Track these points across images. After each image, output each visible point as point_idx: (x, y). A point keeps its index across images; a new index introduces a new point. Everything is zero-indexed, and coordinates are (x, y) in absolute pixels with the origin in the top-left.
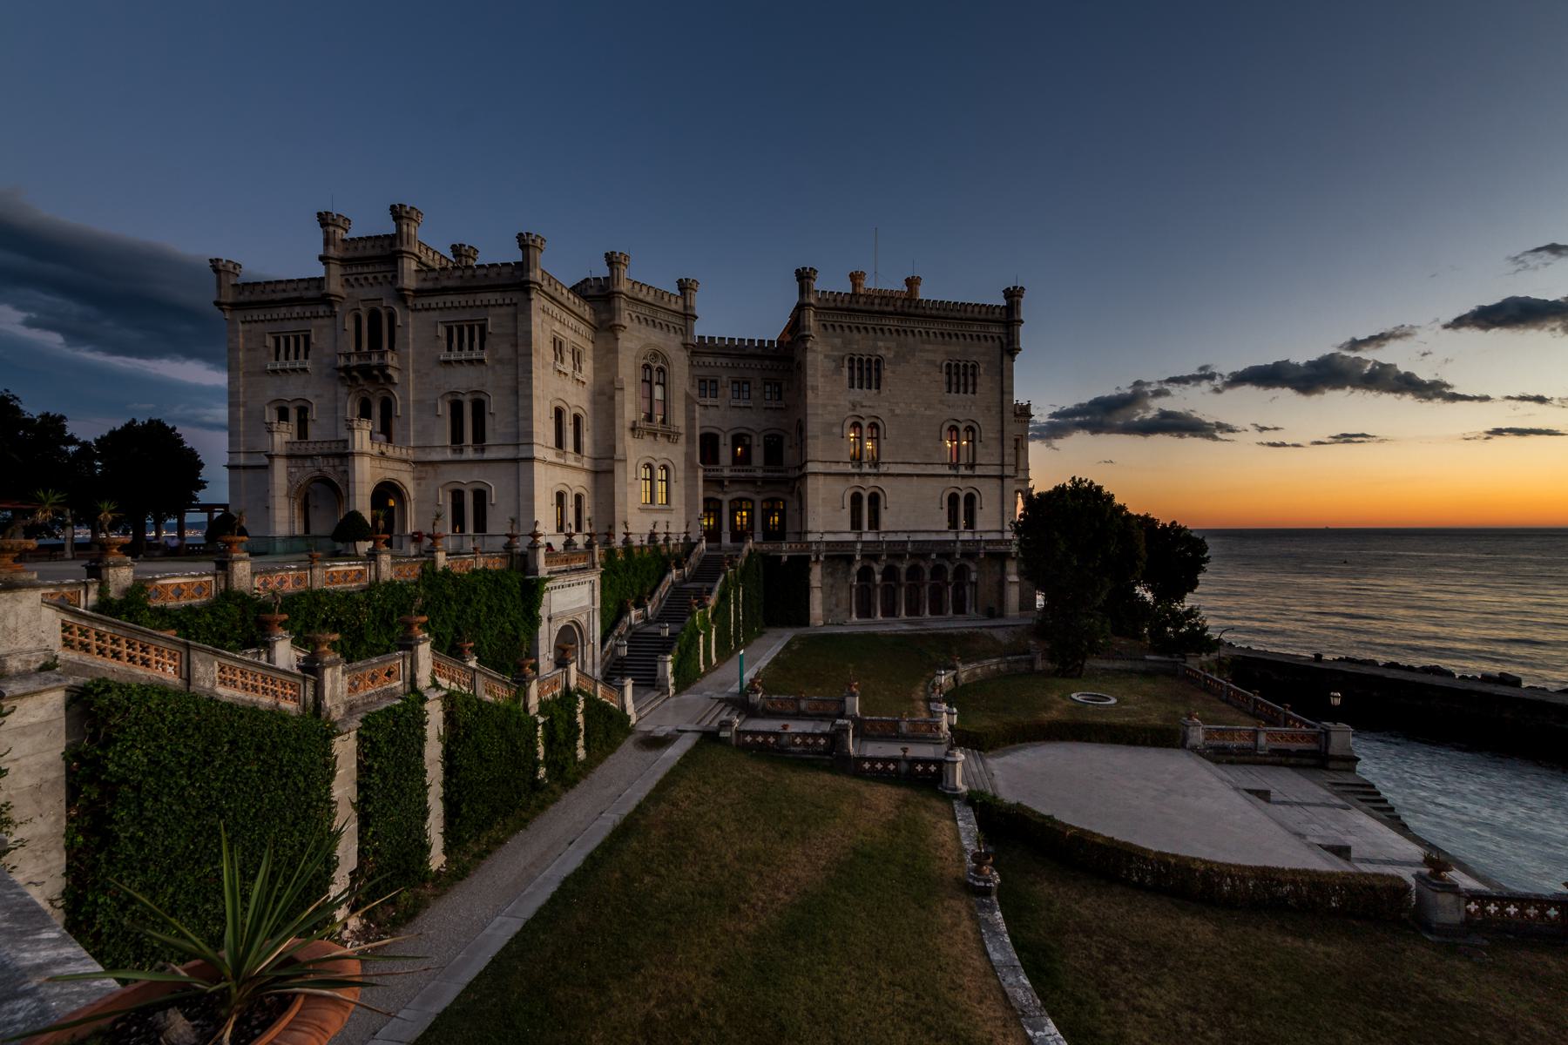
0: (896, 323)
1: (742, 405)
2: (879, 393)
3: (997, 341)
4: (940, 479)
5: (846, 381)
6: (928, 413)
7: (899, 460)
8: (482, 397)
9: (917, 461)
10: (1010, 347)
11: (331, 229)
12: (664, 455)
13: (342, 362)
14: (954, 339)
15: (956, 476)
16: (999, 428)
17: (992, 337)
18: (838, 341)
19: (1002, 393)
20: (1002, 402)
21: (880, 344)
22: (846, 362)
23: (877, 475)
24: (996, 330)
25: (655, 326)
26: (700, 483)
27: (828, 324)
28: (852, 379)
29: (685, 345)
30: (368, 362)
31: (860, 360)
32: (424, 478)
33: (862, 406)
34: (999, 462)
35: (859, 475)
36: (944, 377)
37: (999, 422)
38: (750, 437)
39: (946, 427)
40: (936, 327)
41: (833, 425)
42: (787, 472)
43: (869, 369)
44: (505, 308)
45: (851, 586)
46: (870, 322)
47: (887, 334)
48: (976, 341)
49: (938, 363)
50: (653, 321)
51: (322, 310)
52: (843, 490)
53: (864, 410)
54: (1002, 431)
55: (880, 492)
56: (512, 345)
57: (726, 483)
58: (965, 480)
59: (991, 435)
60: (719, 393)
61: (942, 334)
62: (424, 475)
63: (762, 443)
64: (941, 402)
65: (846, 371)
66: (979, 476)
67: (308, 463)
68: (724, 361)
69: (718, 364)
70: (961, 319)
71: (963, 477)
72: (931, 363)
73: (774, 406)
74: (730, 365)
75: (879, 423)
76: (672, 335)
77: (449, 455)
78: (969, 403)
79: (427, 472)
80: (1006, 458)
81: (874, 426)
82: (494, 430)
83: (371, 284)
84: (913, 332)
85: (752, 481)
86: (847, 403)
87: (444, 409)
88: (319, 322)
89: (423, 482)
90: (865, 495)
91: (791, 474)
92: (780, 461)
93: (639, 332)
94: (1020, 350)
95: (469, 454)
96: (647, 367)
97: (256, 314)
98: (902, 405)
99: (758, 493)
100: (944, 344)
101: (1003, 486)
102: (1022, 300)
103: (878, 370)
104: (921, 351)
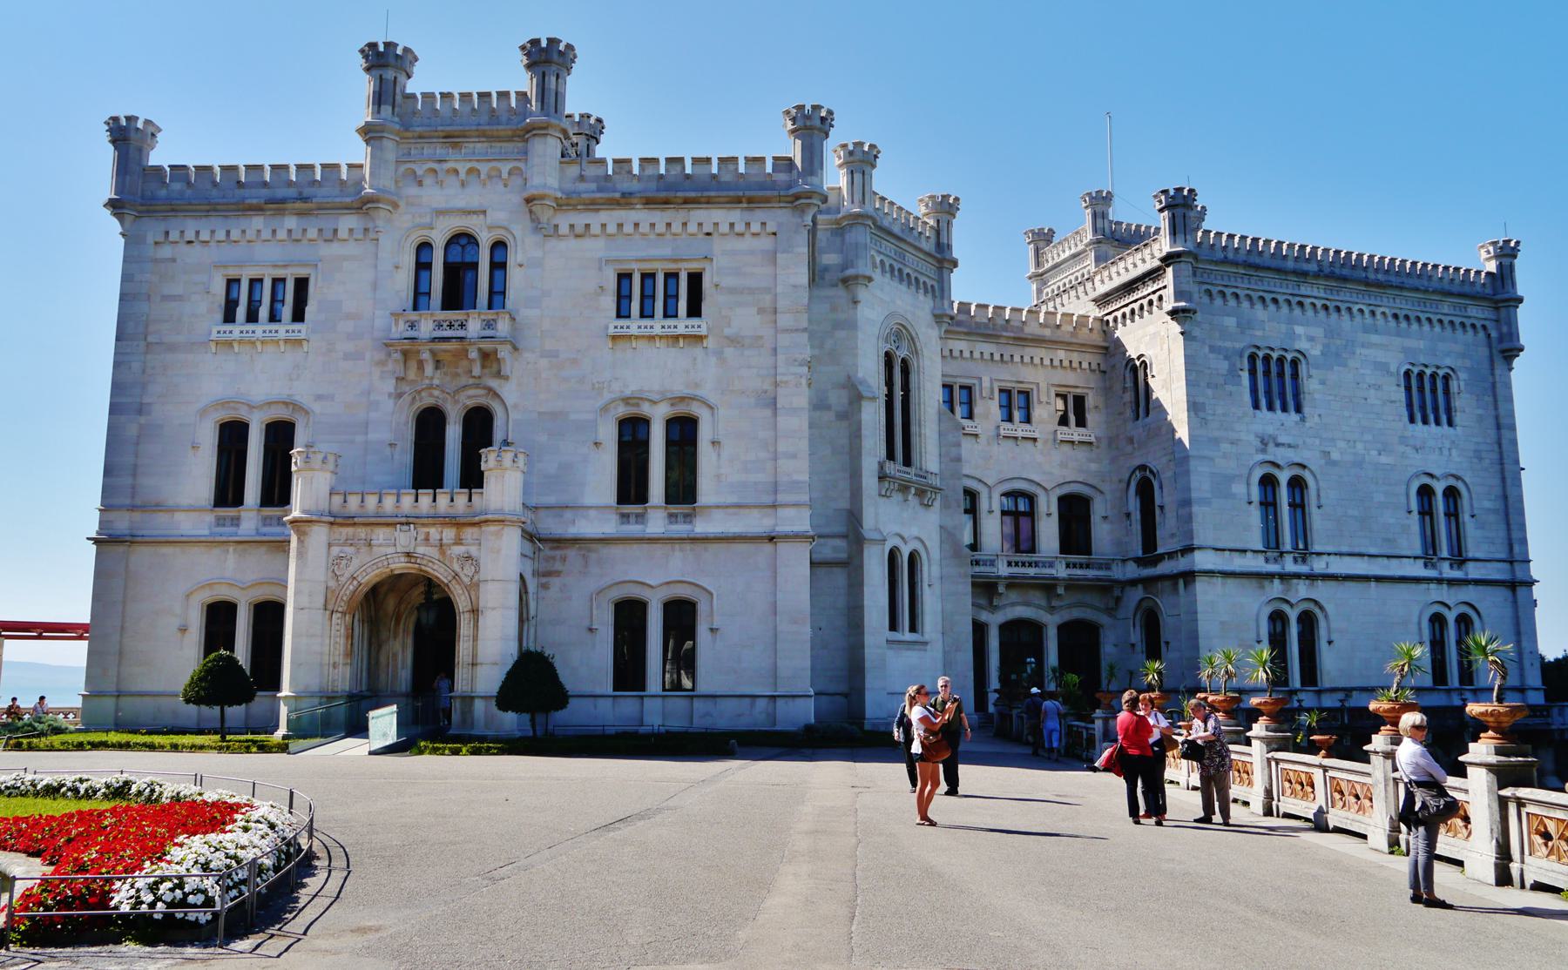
0: (1322, 294)
1: (1020, 434)
2: (1303, 419)
3: (1481, 334)
4: (1413, 586)
5: (1247, 397)
6: (1384, 459)
7: (1345, 549)
8: (696, 410)
9: (1373, 551)
10: (1505, 346)
11: (389, 74)
12: (915, 531)
13: (400, 329)
14: (1415, 326)
15: (1439, 581)
16: (1498, 491)
17: (1473, 326)
19: (1498, 427)
20: (1500, 445)
21: (1299, 330)
23: (1311, 577)
24: (1477, 312)
25: (901, 280)
26: (969, 588)
27: (1214, 290)
29: (938, 318)
30: (461, 333)
31: (1267, 358)
32: (557, 573)
33: (1278, 445)
34: (1503, 556)
35: (1284, 577)
36: (1401, 395)
37: (1497, 481)
38: (1031, 499)
40: (1388, 304)
41: (1231, 479)
42: (1108, 567)
43: (1281, 374)
44: (748, 243)
46: (1284, 289)
47: (1310, 313)
48: (1449, 329)
49: (1393, 368)
50: (900, 270)
51: (347, 222)
52: (1253, 605)
53: (1281, 450)
54: (1505, 497)
55: (1317, 611)
56: (761, 311)
57: (1001, 589)
58: (1454, 590)
59: (1487, 504)
60: (977, 410)
61: (1396, 316)
62: (558, 566)
63: (1054, 509)
64: (1403, 440)
65: (1245, 375)
66: (1477, 582)
67: (381, 534)
68: (988, 348)
69: (977, 355)
70: (1426, 291)
71: (1452, 582)
72: (1382, 367)
73: (1076, 438)
74: (997, 357)
75: (1307, 475)
76: (921, 297)
77: (609, 525)
78: (1447, 445)
79: (564, 559)
80: (1516, 549)
81: (1297, 484)
82: (718, 476)
83: (463, 184)
84: (1349, 309)
85: (1048, 587)
86: (1252, 437)
87: (609, 434)
88: (335, 249)
89: (555, 582)
90: (1293, 615)
91: (1117, 573)
92: (1089, 553)
93: (882, 290)
94: (1522, 350)
95: (657, 521)
96: (889, 359)
97: (191, 227)
98: (1341, 444)
99: (1051, 609)
100: (1398, 334)
101: (1515, 602)
102: (1516, 262)
103: (1295, 375)
104: (1363, 346)
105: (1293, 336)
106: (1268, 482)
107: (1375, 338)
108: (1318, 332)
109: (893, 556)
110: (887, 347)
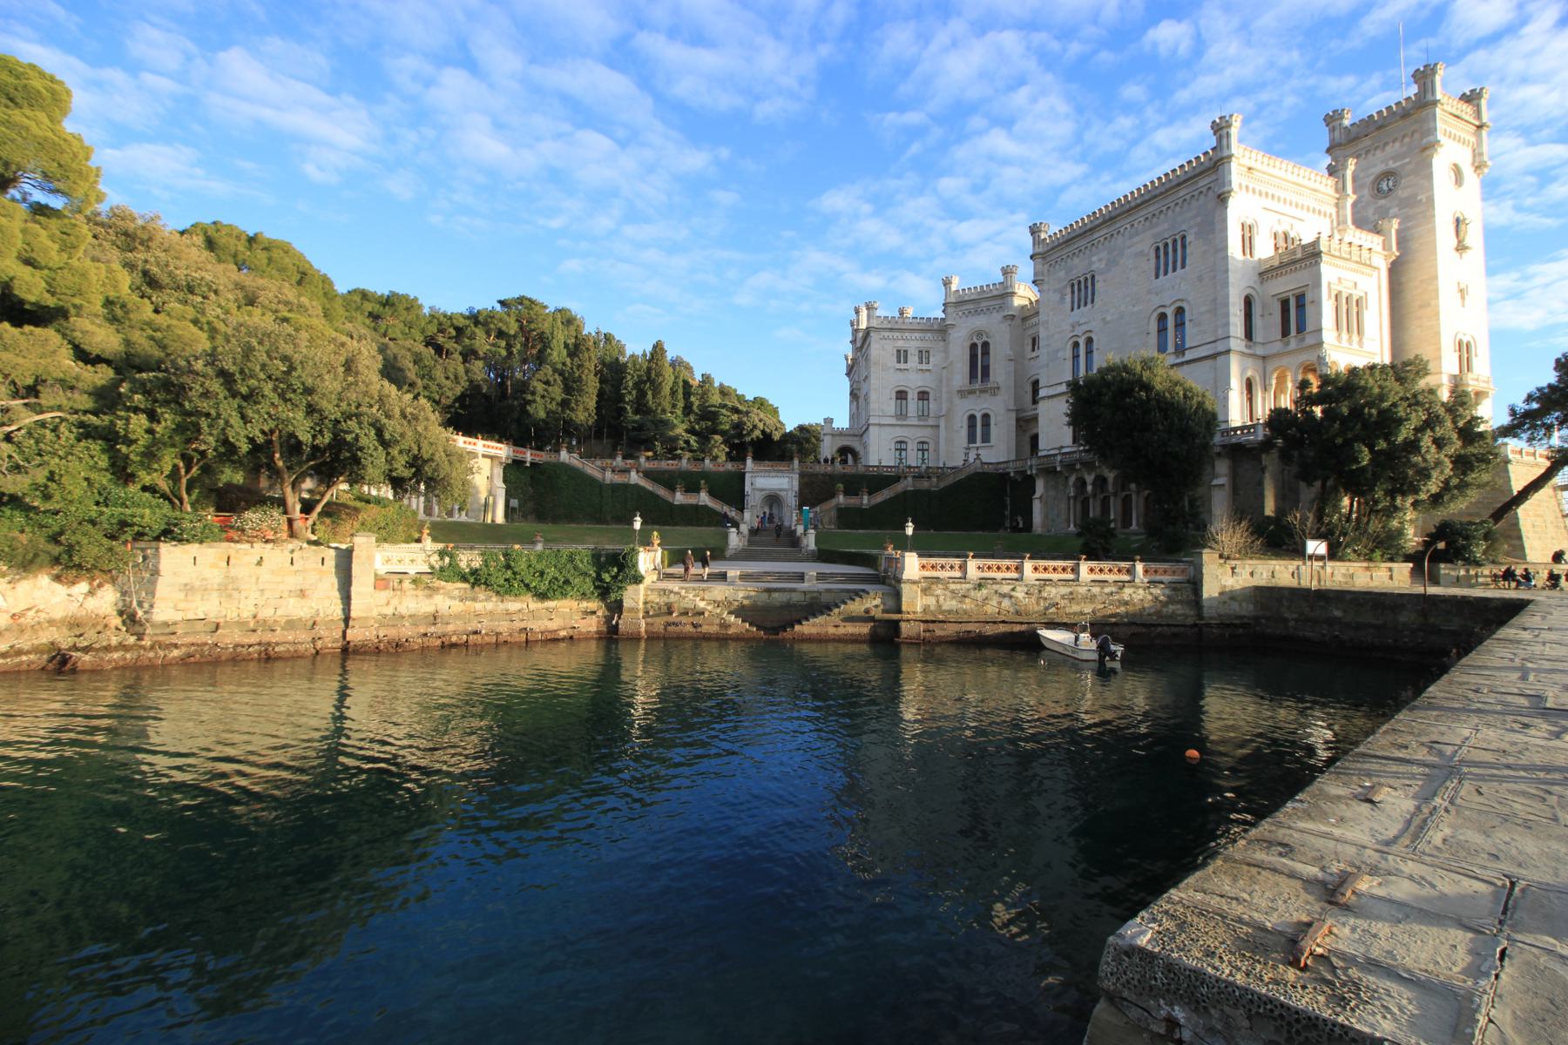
6: (1136, 309)
18: (1062, 274)
21: (1094, 259)
22: (1069, 290)
26: (1014, 422)
28: (1073, 303)
39: (1155, 315)
41: (1058, 351)
45: (1069, 498)
46: (1082, 242)
54: (1215, 300)
59: (1203, 309)
64: (1149, 292)
65: (1068, 298)
81: (1089, 341)
96: (973, 346)
103: (1093, 284)
105: (1091, 263)
106: (1076, 345)
107: (1136, 239)
108: (1104, 254)
109: (972, 418)
110: (967, 344)
